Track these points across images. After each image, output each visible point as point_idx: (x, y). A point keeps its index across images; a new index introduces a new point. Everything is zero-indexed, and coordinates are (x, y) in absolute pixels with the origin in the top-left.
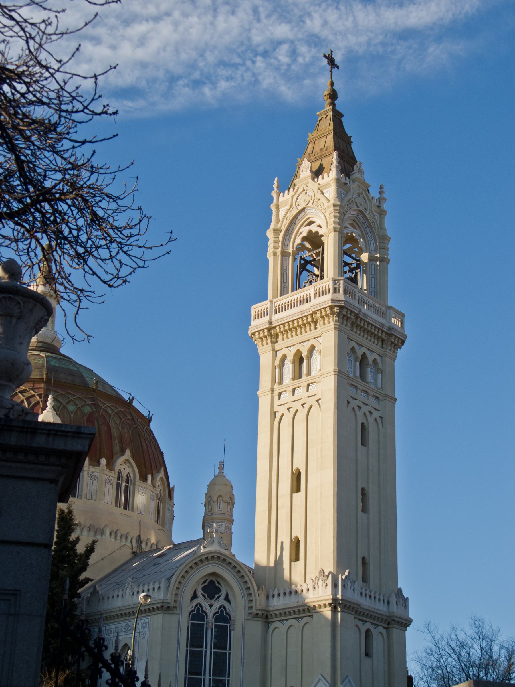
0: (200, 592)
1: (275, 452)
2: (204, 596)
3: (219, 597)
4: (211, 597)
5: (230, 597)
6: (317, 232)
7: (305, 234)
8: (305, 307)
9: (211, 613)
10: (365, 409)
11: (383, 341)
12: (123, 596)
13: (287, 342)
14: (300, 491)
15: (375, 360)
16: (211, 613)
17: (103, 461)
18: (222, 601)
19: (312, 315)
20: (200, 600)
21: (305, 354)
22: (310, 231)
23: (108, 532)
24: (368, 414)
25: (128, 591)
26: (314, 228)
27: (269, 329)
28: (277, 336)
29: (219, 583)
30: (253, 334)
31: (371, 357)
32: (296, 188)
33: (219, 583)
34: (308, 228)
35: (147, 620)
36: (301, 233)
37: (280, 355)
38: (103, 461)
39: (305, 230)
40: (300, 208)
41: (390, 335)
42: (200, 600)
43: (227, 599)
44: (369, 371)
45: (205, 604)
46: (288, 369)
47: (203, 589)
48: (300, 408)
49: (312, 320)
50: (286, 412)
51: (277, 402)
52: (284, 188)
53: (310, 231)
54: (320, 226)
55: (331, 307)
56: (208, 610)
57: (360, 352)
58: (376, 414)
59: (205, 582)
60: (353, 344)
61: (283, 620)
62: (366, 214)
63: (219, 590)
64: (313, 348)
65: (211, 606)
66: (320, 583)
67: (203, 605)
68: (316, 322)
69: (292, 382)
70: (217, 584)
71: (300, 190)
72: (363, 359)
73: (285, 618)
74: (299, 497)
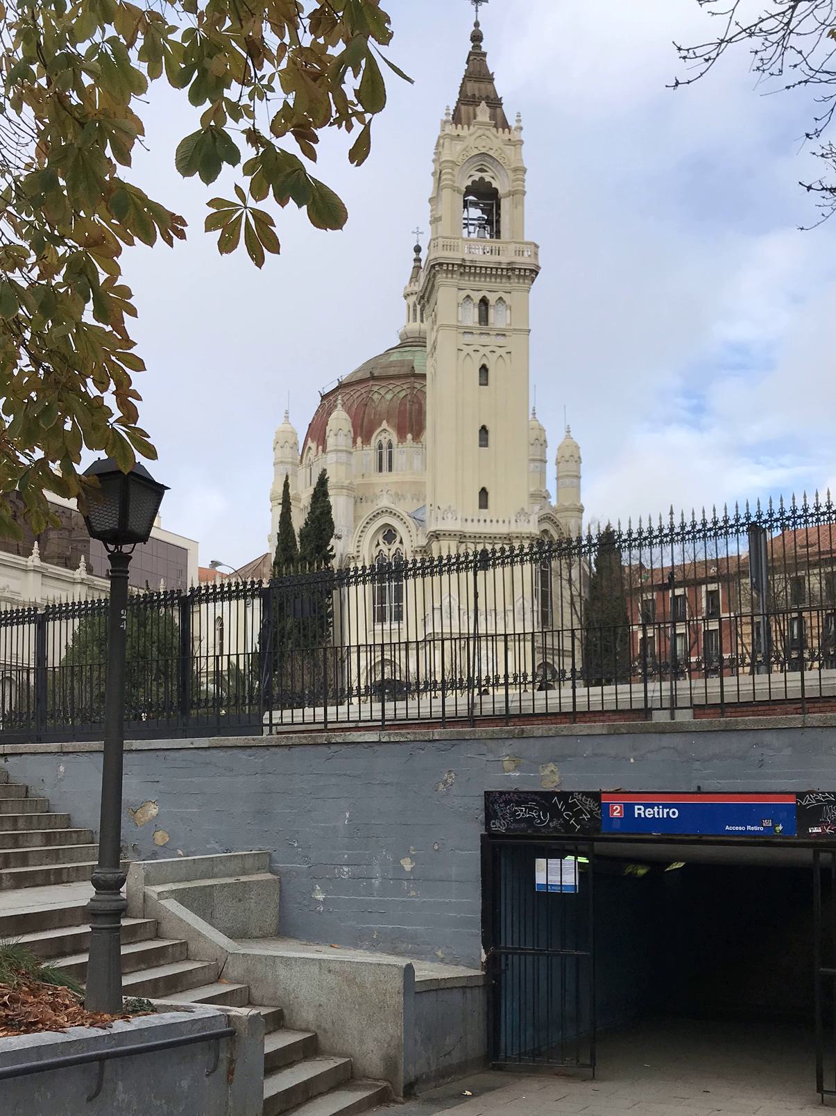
10: (486, 350)
11: (509, 277)
15: (501, 298)
17: (409, 436)
18: (397, 545)
20: (382, 546)
23: (409, 496)
24: (488, 354)
31: (492, 298)
38: (409, 436)
41: (513, 269)
42: (382, 546)
43: (401, 542)
44: (491, 311)
47: (384, 538)
57: (476, 297)
58: (502, 351)
60: (463, 294)
62: (491, 153)
63: (395, 536)
72: (484, 302)
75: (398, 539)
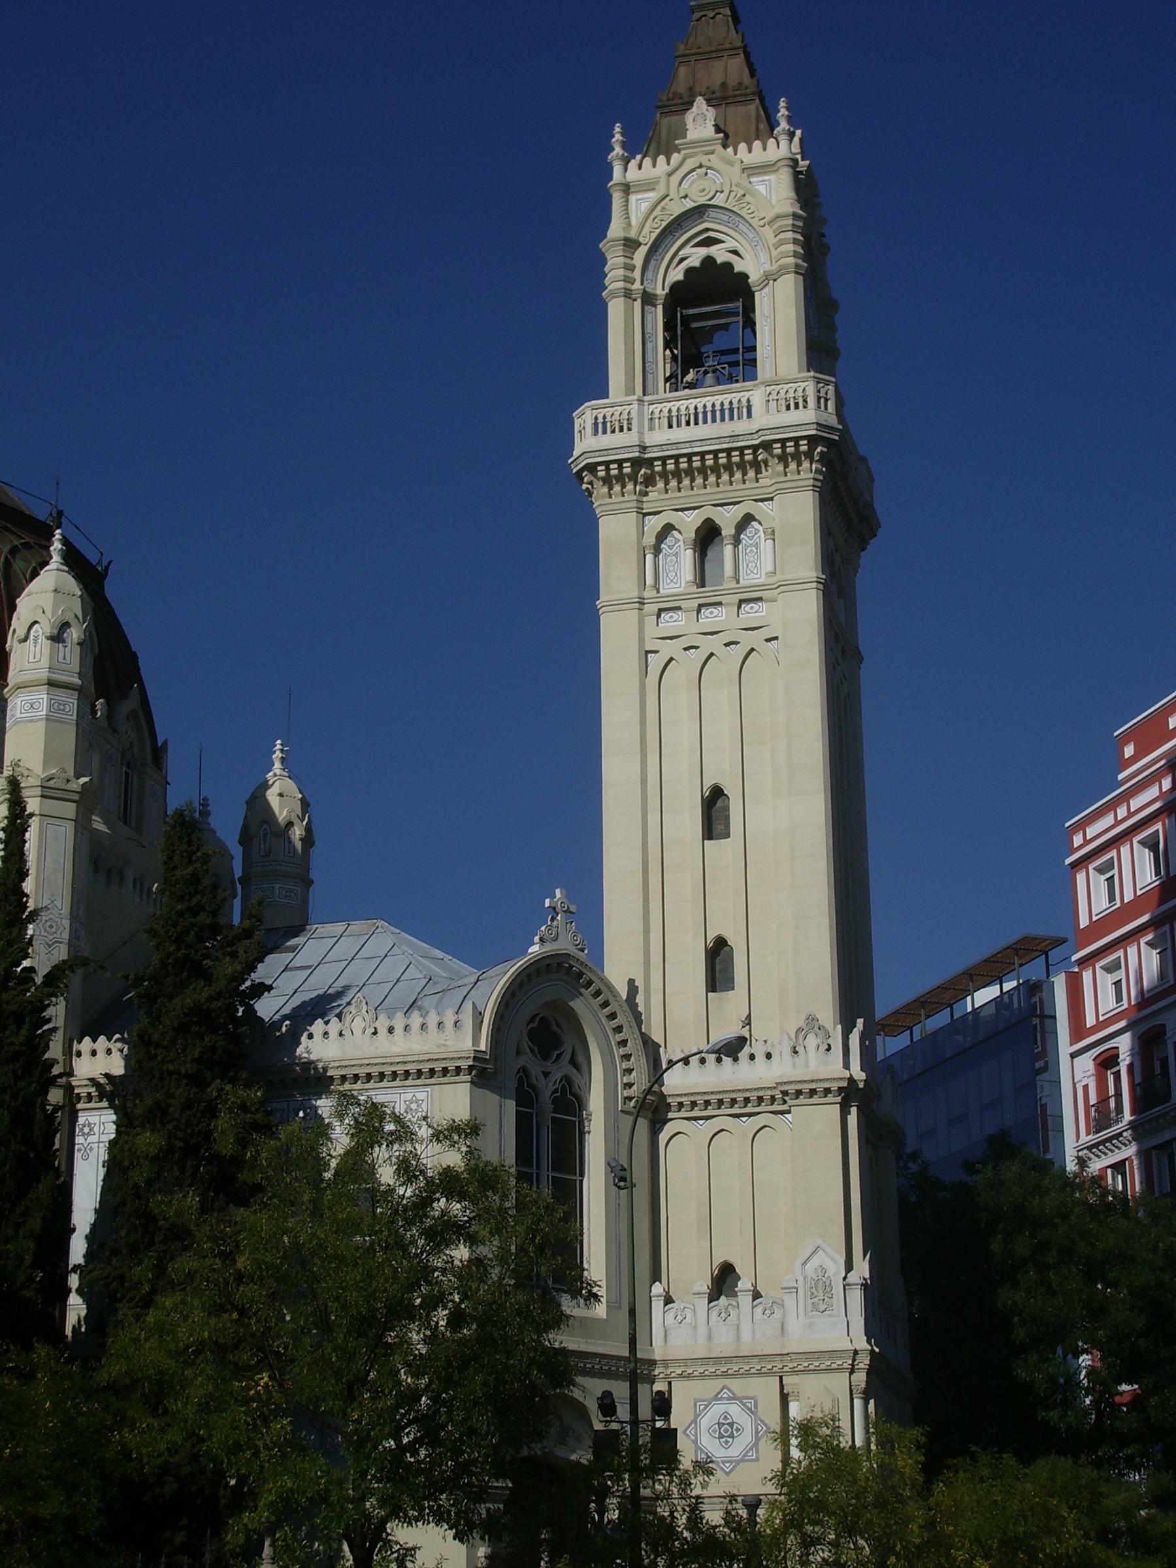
0: (526, 1042)
1: (651, 742)
2: (532, 1050)
3: (559, 1056)
4: (545, 1056)
5: (580, 1059)
6: (728, 266)
7: (695, 261)
8: (741, 426)
9: (547, 1089)
12: (341, 1035)
13: (675, 497)
14: (727, 835)
16: (547, 1089)
19: (755, 448)
21: (728, 531)
22: (709, 261)
25: (358, 1025)
26: (720, 254)
27: (637, 463)
28: (649, 481)
29: (558, 1026)
30: (592, 468)
32: (676, 158)
33: (558, 1026)
34: (703, 252)
35: (421, 1095)
36: (682, 260)
37: (654, 524)
39: (695, 256)
40: (689, 204)
43: (573, 1062)
45: (535, 1070)
46: (680, 561)
47: (531, 1034)
48: (719, 650)
49: (747, 459)
50: (679, 655)
51: (651, 630)
52: (636, 147)
53: (709, 261)
54: (735, 252)
55: (809, 438)
56: (541, 1083)
59: (532, 1020)
61: (696, 1119)
63: (556, 1042)
64: (748, 519)
65: (546, 1074)
66: (812, 1041)
67: (533, 1072)
68: (756, 465)
69: (694, 589)
70: (555, 1027)
71: (690, 164)
73: (704, 1113)
74: (722, 851)
75: (567, 1048)
